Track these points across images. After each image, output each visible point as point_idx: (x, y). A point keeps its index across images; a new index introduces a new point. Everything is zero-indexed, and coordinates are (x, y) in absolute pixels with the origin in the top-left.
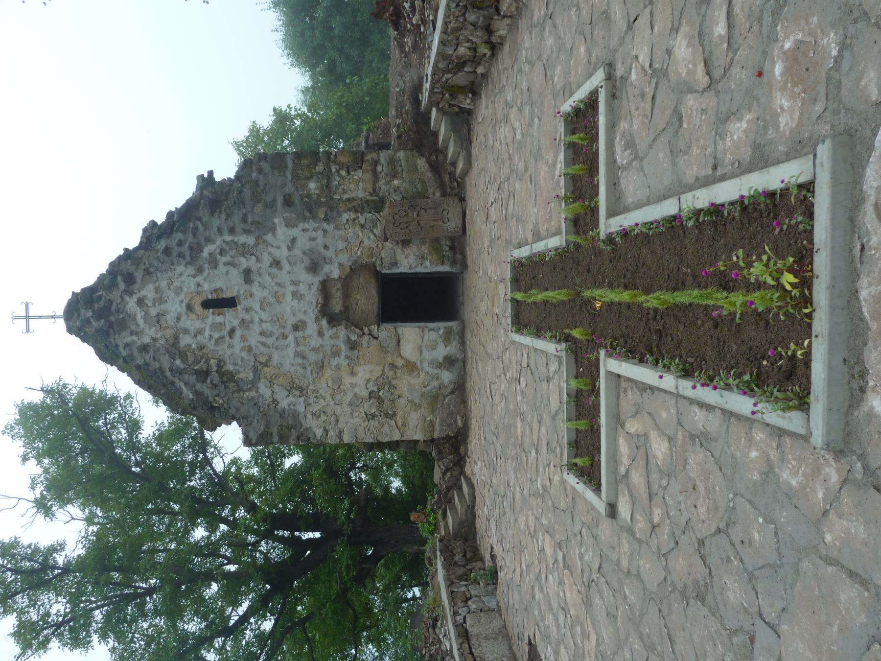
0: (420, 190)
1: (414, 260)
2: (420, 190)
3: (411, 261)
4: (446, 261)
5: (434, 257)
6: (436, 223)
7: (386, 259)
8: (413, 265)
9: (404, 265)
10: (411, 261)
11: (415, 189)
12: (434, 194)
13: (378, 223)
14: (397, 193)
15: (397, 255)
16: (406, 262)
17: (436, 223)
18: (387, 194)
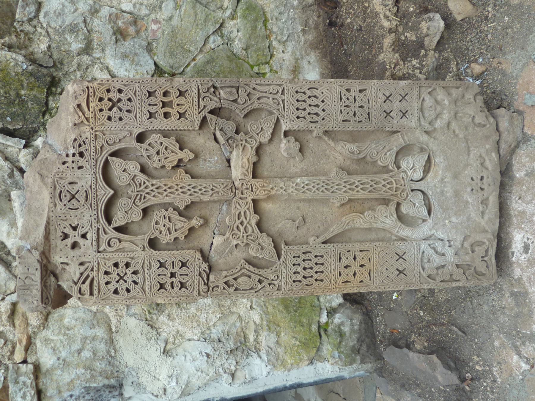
0: (238, 46)
1: (202, 362)
2: (238, 46)
3: (190, 367)
4: (327, 349)
5: (285, 337)
6: (359, 222)
7: (67, 378)
8: (196, 382)
9: (156, 387)
10: (190, 367)
11: (215, 41)
12: (296, 70)
13: (14, 194)
14: (128, 44)
15: (121, 342)
16: (163, 373)
17: (359, 222)
18: (76, 46)
